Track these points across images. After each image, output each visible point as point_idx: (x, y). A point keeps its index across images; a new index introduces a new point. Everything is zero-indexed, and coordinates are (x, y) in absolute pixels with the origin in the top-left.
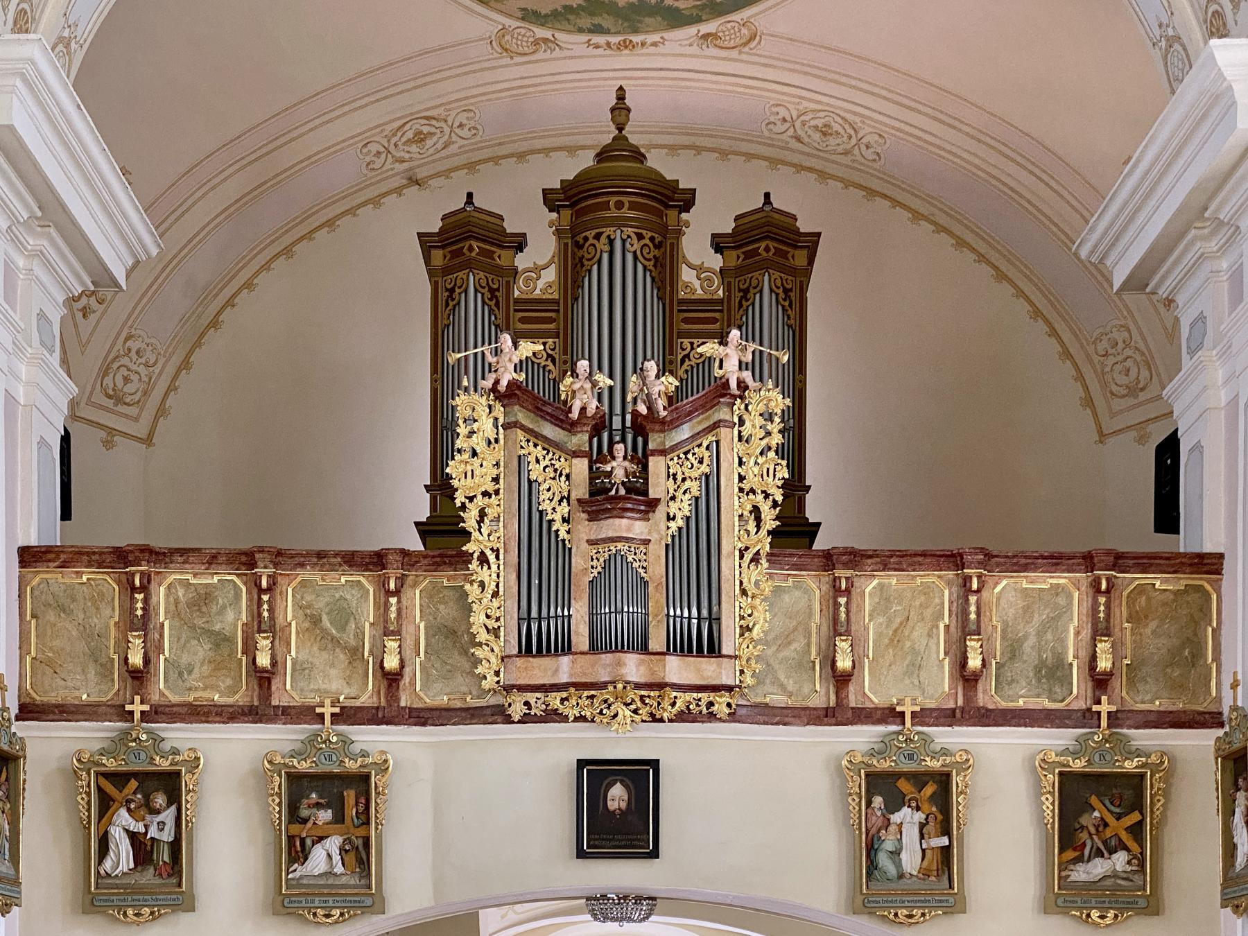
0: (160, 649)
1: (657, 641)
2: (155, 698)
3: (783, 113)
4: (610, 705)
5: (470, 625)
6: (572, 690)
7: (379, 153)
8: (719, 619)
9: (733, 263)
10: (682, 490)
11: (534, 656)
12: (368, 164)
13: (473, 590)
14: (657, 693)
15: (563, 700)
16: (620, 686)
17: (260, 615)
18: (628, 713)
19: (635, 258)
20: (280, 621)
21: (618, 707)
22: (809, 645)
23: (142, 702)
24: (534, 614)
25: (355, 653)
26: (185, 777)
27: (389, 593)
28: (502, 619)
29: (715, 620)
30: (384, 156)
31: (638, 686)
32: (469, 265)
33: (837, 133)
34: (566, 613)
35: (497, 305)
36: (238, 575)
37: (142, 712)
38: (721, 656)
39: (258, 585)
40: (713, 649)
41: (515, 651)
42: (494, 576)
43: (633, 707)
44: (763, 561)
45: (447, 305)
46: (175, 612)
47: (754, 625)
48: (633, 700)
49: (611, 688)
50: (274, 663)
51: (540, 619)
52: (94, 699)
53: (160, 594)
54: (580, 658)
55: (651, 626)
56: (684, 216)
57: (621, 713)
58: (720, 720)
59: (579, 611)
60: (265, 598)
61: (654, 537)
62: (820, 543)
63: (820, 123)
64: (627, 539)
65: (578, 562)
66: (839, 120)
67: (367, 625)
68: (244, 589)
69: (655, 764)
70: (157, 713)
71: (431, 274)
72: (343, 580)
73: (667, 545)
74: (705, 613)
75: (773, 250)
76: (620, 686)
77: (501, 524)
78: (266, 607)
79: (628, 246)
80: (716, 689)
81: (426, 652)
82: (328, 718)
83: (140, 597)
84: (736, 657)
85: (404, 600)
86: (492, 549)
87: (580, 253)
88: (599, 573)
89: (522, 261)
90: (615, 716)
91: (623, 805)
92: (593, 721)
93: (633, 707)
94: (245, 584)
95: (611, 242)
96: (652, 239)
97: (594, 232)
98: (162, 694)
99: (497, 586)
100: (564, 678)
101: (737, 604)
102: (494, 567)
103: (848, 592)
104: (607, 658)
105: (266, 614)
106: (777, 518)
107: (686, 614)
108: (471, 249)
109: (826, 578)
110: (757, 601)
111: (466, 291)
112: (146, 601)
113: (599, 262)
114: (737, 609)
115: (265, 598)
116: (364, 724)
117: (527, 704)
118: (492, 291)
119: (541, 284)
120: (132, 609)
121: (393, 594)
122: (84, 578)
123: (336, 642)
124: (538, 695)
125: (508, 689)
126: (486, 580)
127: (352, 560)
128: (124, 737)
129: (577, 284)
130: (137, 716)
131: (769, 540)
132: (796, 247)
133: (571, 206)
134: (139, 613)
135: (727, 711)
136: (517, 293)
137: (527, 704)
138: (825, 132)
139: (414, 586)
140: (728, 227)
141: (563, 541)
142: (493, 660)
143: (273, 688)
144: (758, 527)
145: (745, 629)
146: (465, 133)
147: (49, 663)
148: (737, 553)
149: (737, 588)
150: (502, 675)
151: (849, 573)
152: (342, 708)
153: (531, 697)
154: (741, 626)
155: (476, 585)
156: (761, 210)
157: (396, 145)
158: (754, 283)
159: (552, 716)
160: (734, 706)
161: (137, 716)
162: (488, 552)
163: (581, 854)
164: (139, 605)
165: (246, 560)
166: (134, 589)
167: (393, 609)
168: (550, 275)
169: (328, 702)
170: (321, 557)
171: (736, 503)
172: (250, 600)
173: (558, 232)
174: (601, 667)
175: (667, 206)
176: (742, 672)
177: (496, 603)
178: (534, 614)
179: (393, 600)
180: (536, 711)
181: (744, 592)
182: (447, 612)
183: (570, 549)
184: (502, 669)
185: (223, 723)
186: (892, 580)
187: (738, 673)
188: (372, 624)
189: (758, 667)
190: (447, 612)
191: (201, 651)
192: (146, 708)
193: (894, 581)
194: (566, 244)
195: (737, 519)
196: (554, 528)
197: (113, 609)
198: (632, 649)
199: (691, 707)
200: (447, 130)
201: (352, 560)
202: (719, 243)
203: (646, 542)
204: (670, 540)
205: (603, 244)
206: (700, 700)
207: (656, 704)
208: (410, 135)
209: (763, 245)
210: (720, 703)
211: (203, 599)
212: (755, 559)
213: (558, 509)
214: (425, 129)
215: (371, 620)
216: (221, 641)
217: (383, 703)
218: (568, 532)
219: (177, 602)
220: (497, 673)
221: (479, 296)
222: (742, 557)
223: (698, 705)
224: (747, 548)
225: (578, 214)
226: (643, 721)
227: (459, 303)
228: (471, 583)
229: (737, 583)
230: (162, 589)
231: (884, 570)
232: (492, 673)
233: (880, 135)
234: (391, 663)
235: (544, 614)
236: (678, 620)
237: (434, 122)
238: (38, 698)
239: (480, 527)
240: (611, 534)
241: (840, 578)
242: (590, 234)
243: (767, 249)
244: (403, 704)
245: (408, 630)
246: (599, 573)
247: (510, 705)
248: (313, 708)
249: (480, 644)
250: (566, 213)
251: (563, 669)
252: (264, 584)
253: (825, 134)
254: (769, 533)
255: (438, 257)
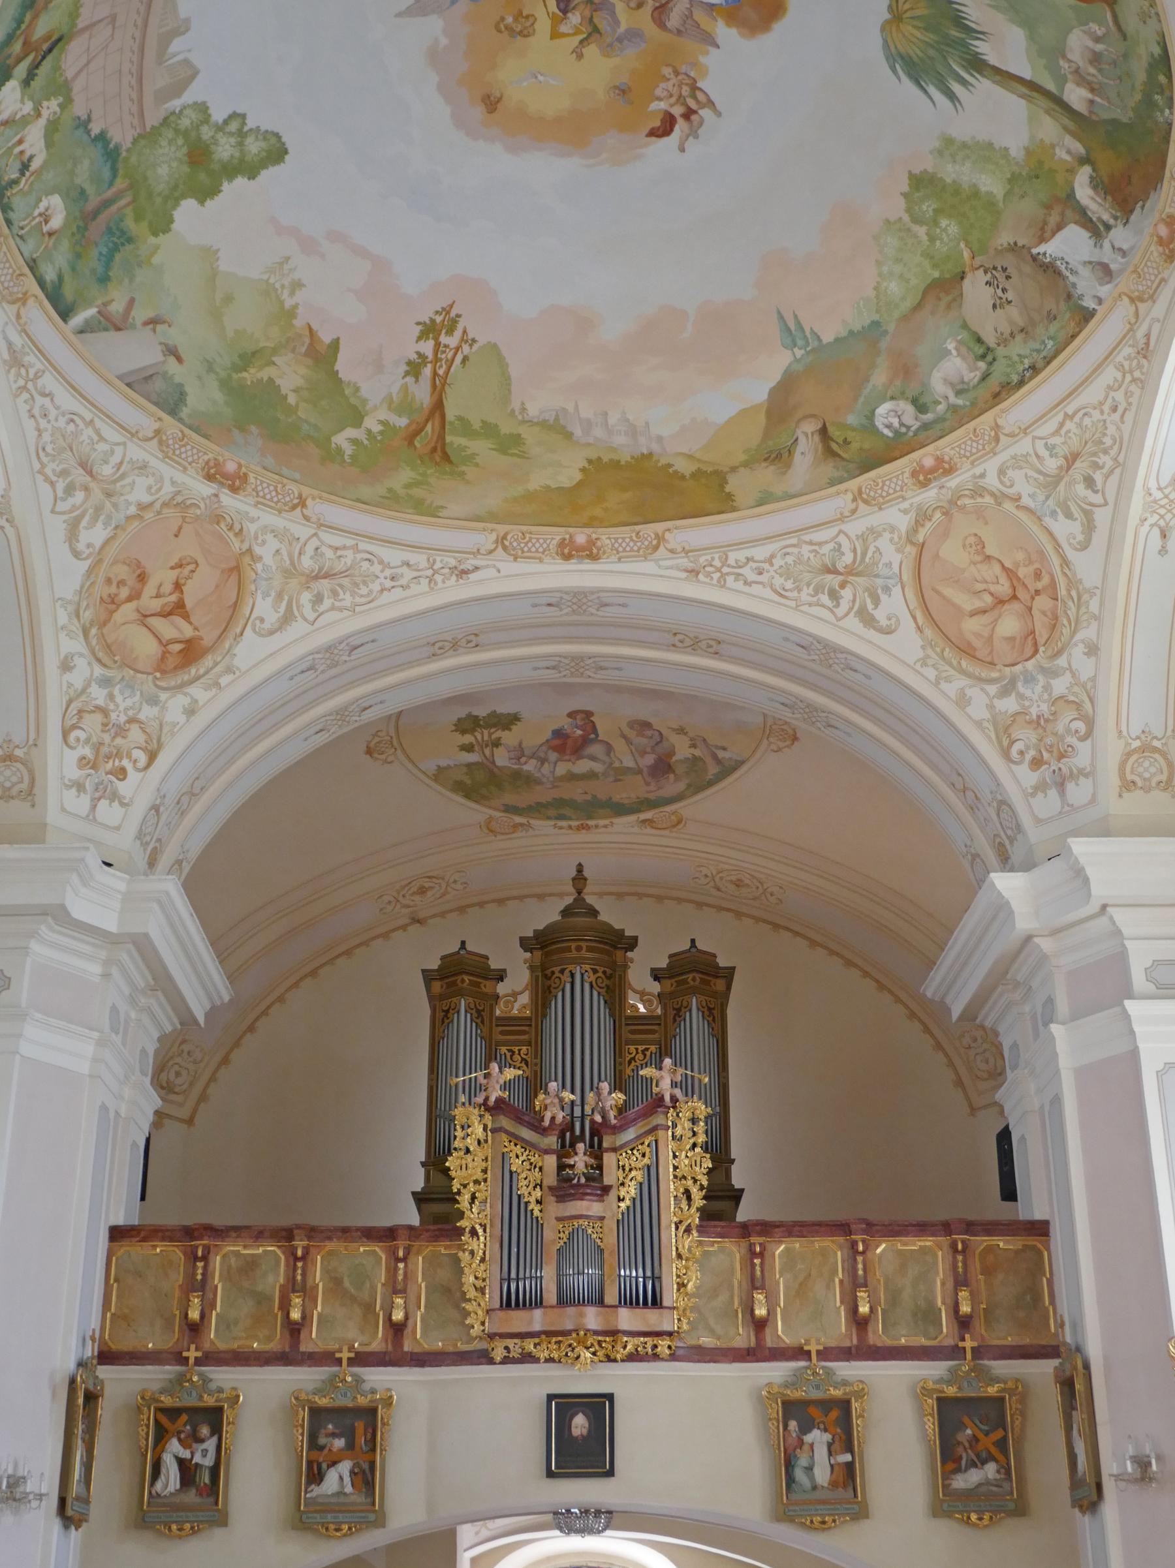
0: (213, 1306)
1: (611, 1297)
2: (207, 1346)
3: (705, 871)
4: (573, 1349)
5: (462, 1285)
6: (543, 1337)
7: (390, 902)
8: (660, 1278)
9: (668, 989)
10: (630, 1177)
11: (513, 1310)
12: (381, 910)
13: (465, 1257)
14: (612, 1339)
15: (535, 1345)
16: (582, 1333)
17: (294, 1277)
18: (588, 1355)
19: (592, 987)
20: (310, 1283)
21: (580, 1350)
22: (732, 1297)
23: (197, 1349)
24: (513, 1275)
25: (369, 1308)
26: (227, 1413)
27: (399, 1260)
28: (487, 1280)
29: (656, 1279)
30: (393, 904)
31: (596, 1333)
32: (461, 993)
33: (748, 885)
34: (538, 1275)
35: (483, 1022)
36: (279, 1247)
37: (196, 1358)
38: (661, 1307)
39: (294, 1255)
40: (656, 1302)
41: (498, 1305)
42: (482, 1246)
43: (592, 1350)
44: (695, 1233)
45: (443, 1022)
46: (227, 1276)
47: (688, 1282)
48: (592, 1345)
49: (574, 1335)
50: (304, 1317)
51: (518, 1279)
52: (159, 1347)
53: (217, 1261)
54: (549, 1310)
55: (606, 1287)
56: (629, 954)
57: (582, 1354)
58: (663, 1359)
59: (549, 1274)
60: (300, 1264)
61: (608, 1215)
62: (742, 1215)
63: (734, 878)
64: (587, 1217)
65: (549, 1234)
66: (748, 876)
67: (379, 1286)
68: (283, 1257)
69: (610, 1397)
70: (211, 1358)
71: (431, 998)
72: (362, 1249)
73: (618, 1221)
74: (649, 1274)
75: (698, 980)
76: (582, 1333)
77: (488, 1205)
78: (299, 1271)
79: (586, 977)
80: (658, 1334)
81: (426, 1307)
82: (345, 1362)
83: (200, 1264)
84: (674, 1308)
85: (410, 1265)
86: (480, 1225)
87: (548, 983)
88: (565, 1243)
89: (502, 989)
90: (578, 1357)
91: (585, 1432)
92: (560, 1362)
93: (592, 1350)
94: (284, 1253)
95: (572, 975)
96: (604, 972)
97: (559, 968)
98: (212, 1342)
99: (484, 1253)
100: (537, 1327)
101: (674, 1265)
102: (482, 1239)
103: (761, 1255)
104: (571, 1311)
105: (299, 1278)
106: (705, 1198)
107: (634, 1274)
108: (463, 981)
109: (744, 1244)
110: (690, 1263)
111: (458, 1012)
112: (205, 1268)
113: (563, 991)
114: (674, 1270)
115: (300, 1264)
116: (373, 1366)
117: (506, 1348)
118: (478, 1011)
119: (517, 1006)
120: (194, 1274)
121: (400, 1260)
122: (158, 1250)
123: (353, 1299)
124: (516, 1341)
125: (492, 1336)
126: (476, 1248)
127: (370, 1234)
128: (181, 1379)
129: (546, 1005)
130: (191, 1361)
131: (698, 1215)
132: (717, 977)
133: (542, 948)
134: (199, 1277)
135: (667, 1352)
136: (498, 1013)
137: (506, 1348)
138: (738, 884)
139: (418, 1253)
140: (663, 963)
141: (537, 1218)
142: (480, 1312)
143: (303, 1335)
144: (690, 1206)
145: (681, 1285)
146: (458, 886)
147: (125, 1318)
148: (673, 1226)
149: (674, 1253)
150: (487, 1324)
151: (761, 1239)
152: (357, 1353)
153: (510, 1343)
154: (678, 1283)
155: (467, 1254)
156: (689, 951)
157: (404, 896)
158: (685, 1004)
159: (527, 1358)
160: (673, 1348)
161: (191, 1361)
162: (478, 1227)
163: (550, 1474)
164: (200, 1271)
165: (285, 1235)
166: (196, 1259)
167: (401, 1272)
168: (525, 999)
169: (345, 1348)
170: (345, 1233)
171: (672, 1187)
172: (287, 1265)
173: (532, 968)
174: (567, 1319)
175: (616, 948)
176: (679, 1320)
177: (483, 1267)
178: (513, 1275)
179: (401, 1265)
180: (515, 1353)
181: (679, 1256)
182: (444, 1275)
183: (542, 1225)
184: (487, 1320)
185: (261, 1366)
186: (797, 1244)
187: (676, 1321)
188: (383, 1285)
189: (692, 1316)
190: (444, 1275)
191: (246, 1308)
192: (199, 1354)
193: (797, 1245)
194: (537, 977)
195: (672, 1199)
196: (530, 1208)
197: (179, 1274)
198: (591, 1302)
199: (639, 1349)
200: (444, 886)
201: (370, 1234)
202: (657, 975)
203: (602, 1218)
204: (620, 1217)
205: (566, 977)
206: (646, 1343)
207: (610, 1347)
208: (415, 889)
209: (691, 976)
210: (662, 1346)
211: (251, 1265)
212: (688, 1230)
213: (533, 1193)
214: (427, 885)
215: (383, 1280)
216: (262, 1299)
217: (390, 1348)
218: (541, 1211)
219: (230, 1267)
220: (483, 1324)
221: (469, 1015)
222: (677, 1228)
223: (644, 1348)
224: (681, 1222)
225: (547, 955)
226: (602, 1361)
227: (452, 1021)
228: (464, 1251)
229: (674, 1249)
230: (218, 1258)
231: (789, 1237)
232: (479, 1323)
233: (781, 887)
234: (398, 1316)
235: (521, 1275)
236: (628, 1279)
237: (434, 880)
238: (113, 1346)
239: (472, 1208)
240: (574, 1213)
241: (754, 1244)
242: (557, 969)
243: (694, 979)
244: (406, 1349)
245: (412, 1290)
246: (565, 1243)
247: (493, 1349)
248: (333, 1353)
249: (470, 1300)
250: (538, 954)
251: (537, 1320)
252: (299, 1253)
253: (738, 886)
254: (698, 1209)
255: (437, 987)
